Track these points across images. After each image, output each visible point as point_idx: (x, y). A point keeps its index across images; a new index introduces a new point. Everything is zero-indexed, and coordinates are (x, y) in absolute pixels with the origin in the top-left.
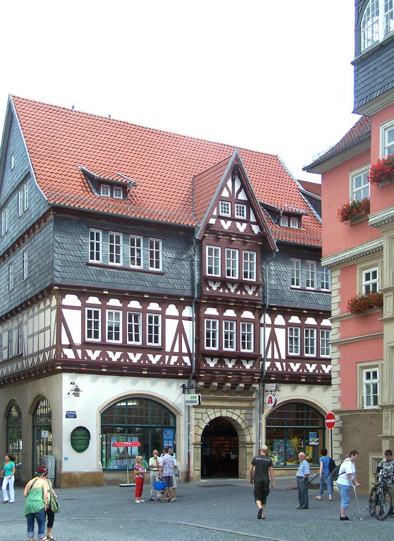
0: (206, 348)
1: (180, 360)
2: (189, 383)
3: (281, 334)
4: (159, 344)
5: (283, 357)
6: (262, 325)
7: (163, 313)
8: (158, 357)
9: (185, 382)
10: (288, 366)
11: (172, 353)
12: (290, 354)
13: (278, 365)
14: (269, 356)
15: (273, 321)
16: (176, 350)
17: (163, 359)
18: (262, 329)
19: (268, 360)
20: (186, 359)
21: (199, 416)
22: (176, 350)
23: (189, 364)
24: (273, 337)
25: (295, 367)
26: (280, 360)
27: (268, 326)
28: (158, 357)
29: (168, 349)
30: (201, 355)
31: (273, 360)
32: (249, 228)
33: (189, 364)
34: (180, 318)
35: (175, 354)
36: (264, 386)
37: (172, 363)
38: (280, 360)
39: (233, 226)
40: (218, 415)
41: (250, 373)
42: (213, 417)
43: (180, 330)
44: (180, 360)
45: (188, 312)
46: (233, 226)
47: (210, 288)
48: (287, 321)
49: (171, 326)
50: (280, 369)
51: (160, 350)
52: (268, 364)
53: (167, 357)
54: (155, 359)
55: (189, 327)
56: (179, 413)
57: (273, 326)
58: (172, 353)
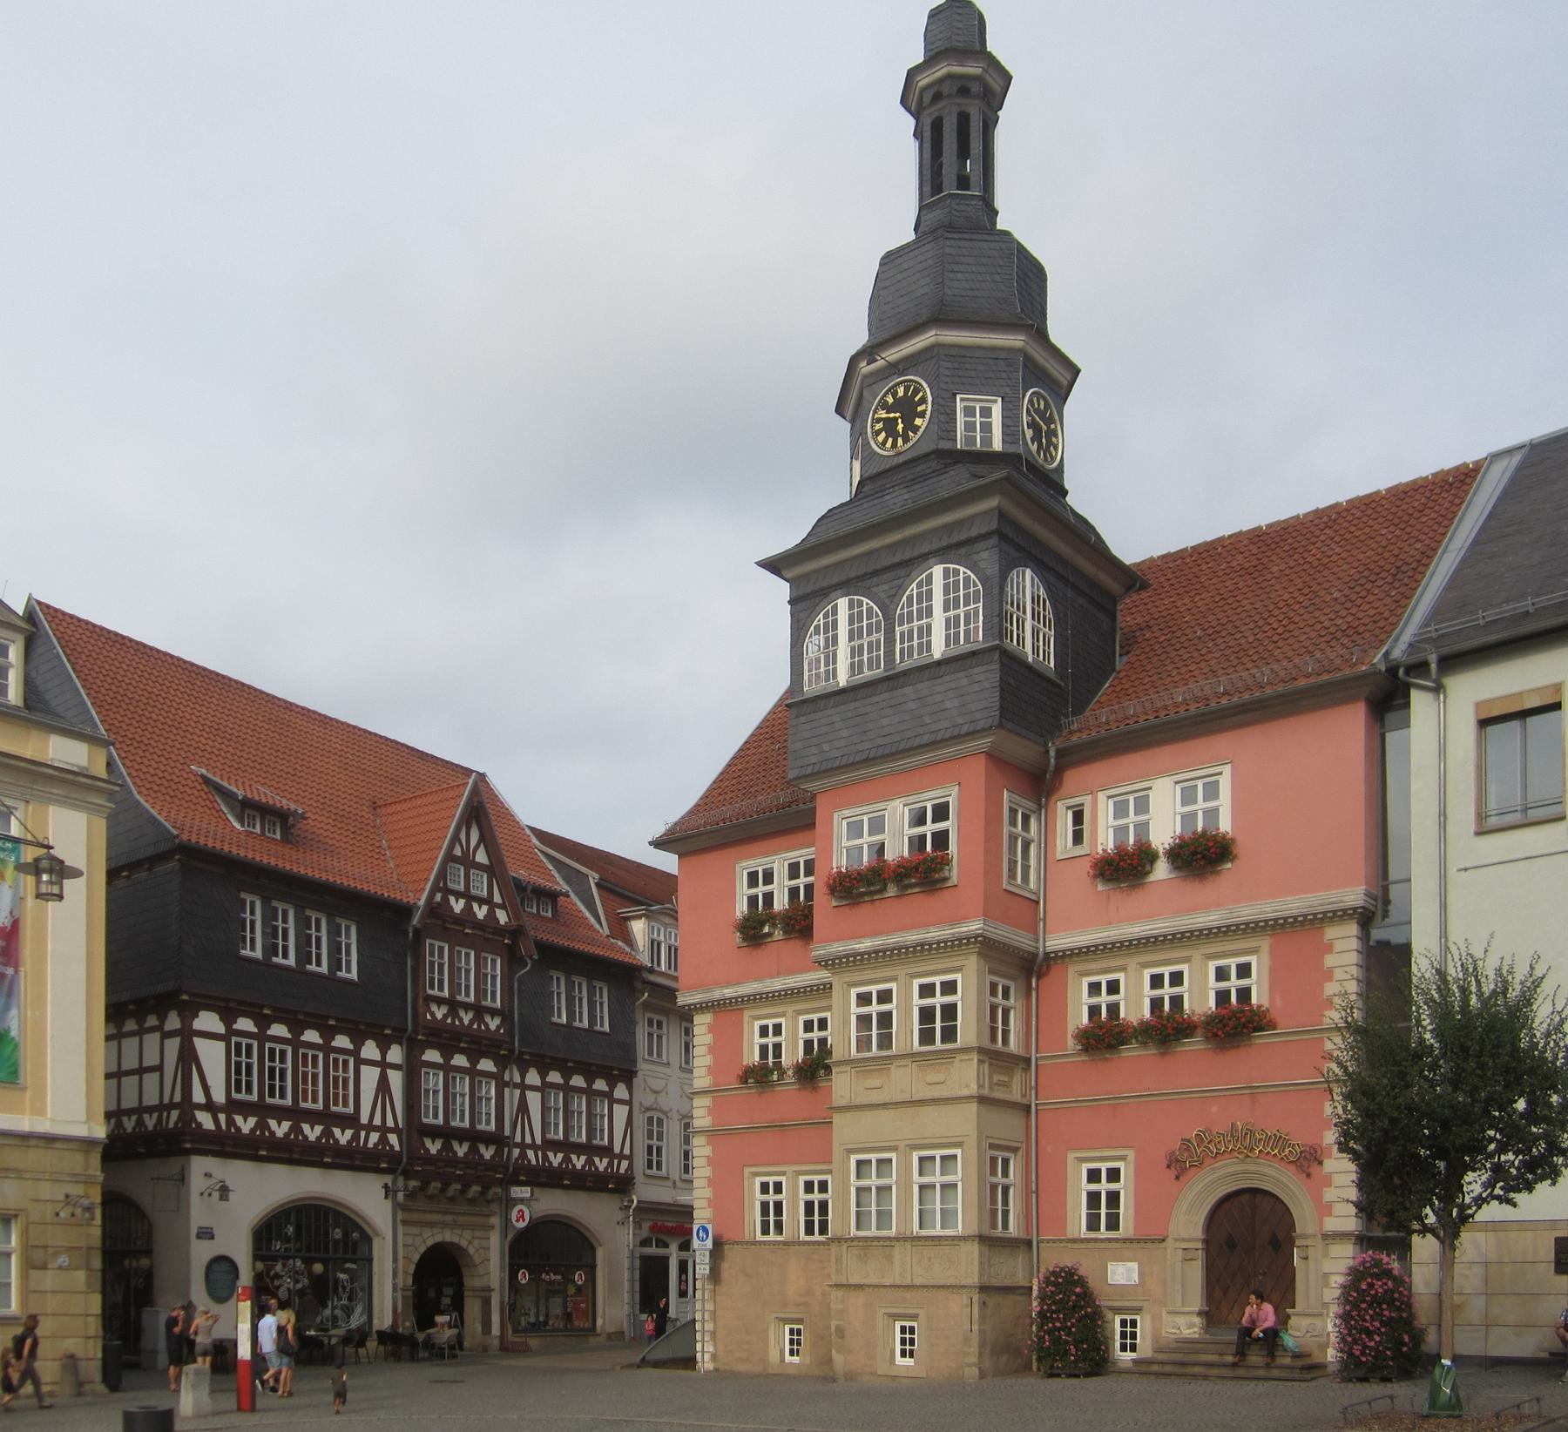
0: (425, 1120)
1: (383, 1140)
2: (394, 1182)
3: (534, 1099)
4: (351, 1109)
5: (539, 1141)
6: (507, 1084)
7: (355, 1053)
8: (349, 1133)
9: (388, 1179)
10: (545, 1158)
11: (370, 1128)
12: (548, 1136)
13: (530, 1154)
14: (518, 1139)
15: (523, 1077)
16: (377, 1121)
17: (356, 1137)
18: (507, 1090)
19: (517, 1145)
20: (393, 1139)
21: (410, 1240)
22: (377, 1121)
23: (397, 1148)
24: (523, 1107)
25: (556, 1159)
26: (533, 1146)
27: (516, 1086)
28: (349, 1133)
29: (364, 1119)
30: (415, 1129)
31: (523, 1146)
32: (491, 914)
33: (397, 1148)
34: (383, 1065)
35: (376, 1129)
36: (508, 1192)
37: (370, 1145)
38: (533, 1146)
39: (468, 909)
40: (438, 1239)
41: (491, 1166)
42: (430, 1243)
43: (383, 1086)
44: (383, 1140)
45: (395, 1054)
46: (468, 909)
47: (433, 1014)
48: (543, 1077)
49: (370, 1076)
50: (534, 1162)
51: (351, 1121)
52: (516, 1152)
53: (363, 1134)
54: (343, 1137)
55: (396, 1079)
56: (378, 1235)
57: (524, 1087)
58: (370, 1128)
